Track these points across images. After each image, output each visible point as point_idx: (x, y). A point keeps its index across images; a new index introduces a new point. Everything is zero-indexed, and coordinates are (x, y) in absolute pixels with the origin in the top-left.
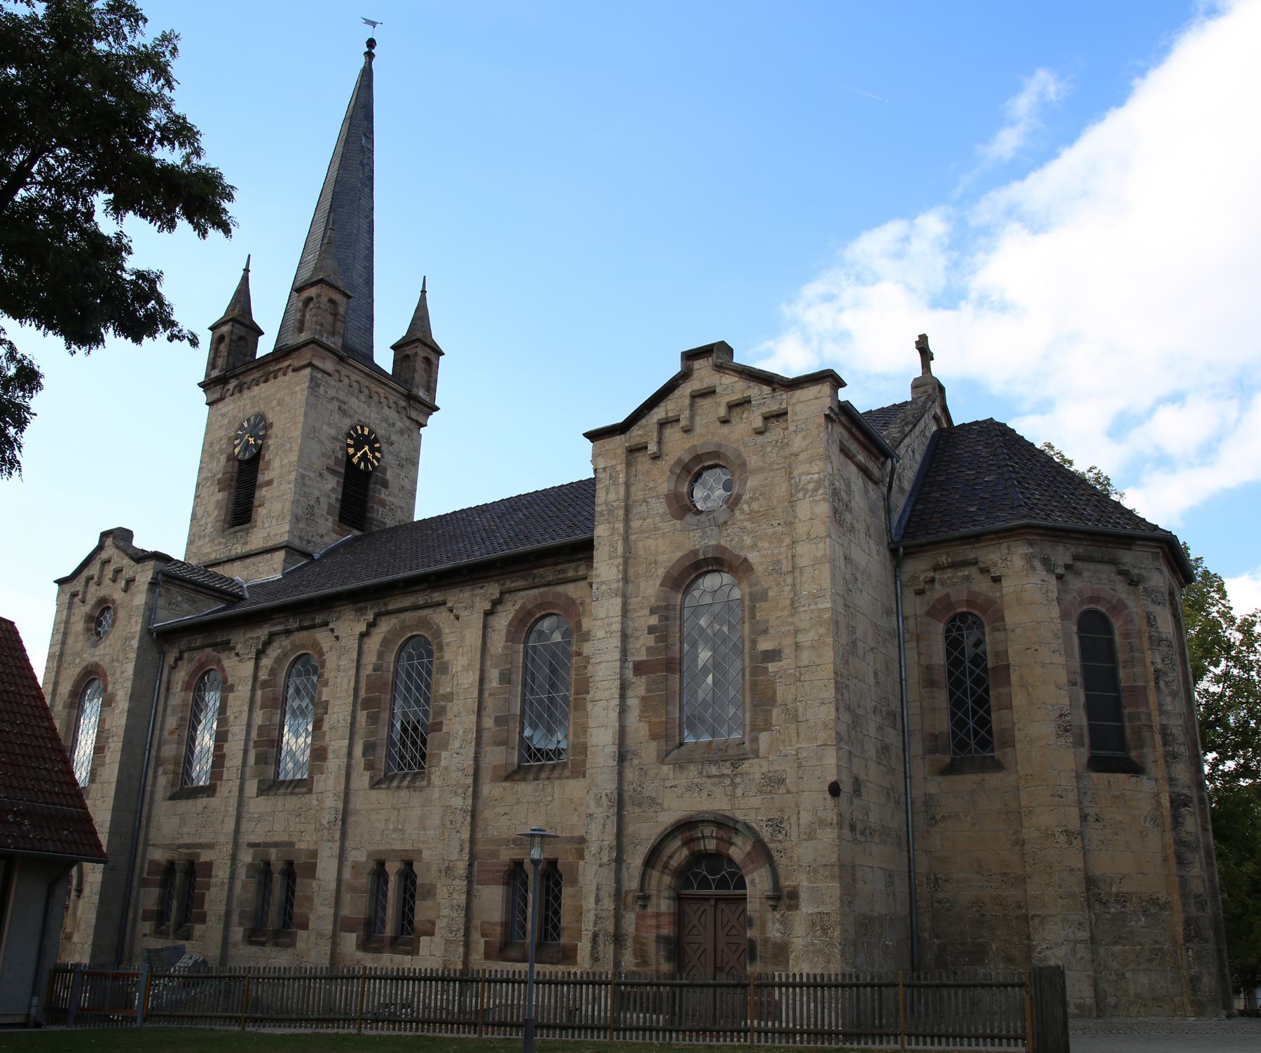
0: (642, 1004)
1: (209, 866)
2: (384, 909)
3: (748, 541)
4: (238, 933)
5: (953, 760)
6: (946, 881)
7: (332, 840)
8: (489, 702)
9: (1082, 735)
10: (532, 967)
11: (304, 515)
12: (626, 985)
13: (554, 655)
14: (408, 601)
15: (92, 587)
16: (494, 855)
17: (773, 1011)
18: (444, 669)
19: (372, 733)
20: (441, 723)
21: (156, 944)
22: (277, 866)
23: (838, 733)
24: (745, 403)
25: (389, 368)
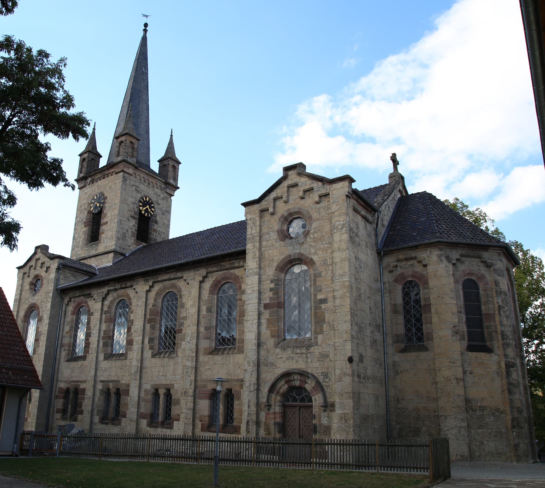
0: (266, 451)
1: (84, 390)
2: (158, 409)
3: (313, 251)
4: (96, 419)
5: (406, 346)
6: (403, 399)
7: (136, 380)
8: (202, 321)
9: (464, 336)
10: (217, 435)
11: (122, 237)
12: (262, 443)
13: (230, 300)
14: (166, 277)
15: (32, 270)
16: (205, 386)
17: (324, 455)
18: (183, 306)
19: (152, 334)
20: (182, 329)
21: (63, 423)
22: (113, 391)
23: (352, 335)
24: (311, 190)
25: (157, 171)
